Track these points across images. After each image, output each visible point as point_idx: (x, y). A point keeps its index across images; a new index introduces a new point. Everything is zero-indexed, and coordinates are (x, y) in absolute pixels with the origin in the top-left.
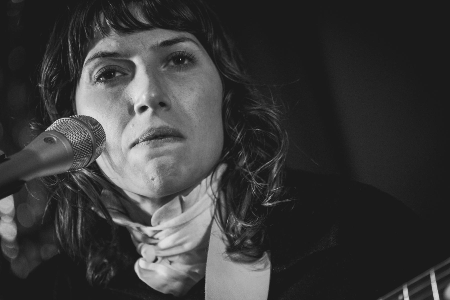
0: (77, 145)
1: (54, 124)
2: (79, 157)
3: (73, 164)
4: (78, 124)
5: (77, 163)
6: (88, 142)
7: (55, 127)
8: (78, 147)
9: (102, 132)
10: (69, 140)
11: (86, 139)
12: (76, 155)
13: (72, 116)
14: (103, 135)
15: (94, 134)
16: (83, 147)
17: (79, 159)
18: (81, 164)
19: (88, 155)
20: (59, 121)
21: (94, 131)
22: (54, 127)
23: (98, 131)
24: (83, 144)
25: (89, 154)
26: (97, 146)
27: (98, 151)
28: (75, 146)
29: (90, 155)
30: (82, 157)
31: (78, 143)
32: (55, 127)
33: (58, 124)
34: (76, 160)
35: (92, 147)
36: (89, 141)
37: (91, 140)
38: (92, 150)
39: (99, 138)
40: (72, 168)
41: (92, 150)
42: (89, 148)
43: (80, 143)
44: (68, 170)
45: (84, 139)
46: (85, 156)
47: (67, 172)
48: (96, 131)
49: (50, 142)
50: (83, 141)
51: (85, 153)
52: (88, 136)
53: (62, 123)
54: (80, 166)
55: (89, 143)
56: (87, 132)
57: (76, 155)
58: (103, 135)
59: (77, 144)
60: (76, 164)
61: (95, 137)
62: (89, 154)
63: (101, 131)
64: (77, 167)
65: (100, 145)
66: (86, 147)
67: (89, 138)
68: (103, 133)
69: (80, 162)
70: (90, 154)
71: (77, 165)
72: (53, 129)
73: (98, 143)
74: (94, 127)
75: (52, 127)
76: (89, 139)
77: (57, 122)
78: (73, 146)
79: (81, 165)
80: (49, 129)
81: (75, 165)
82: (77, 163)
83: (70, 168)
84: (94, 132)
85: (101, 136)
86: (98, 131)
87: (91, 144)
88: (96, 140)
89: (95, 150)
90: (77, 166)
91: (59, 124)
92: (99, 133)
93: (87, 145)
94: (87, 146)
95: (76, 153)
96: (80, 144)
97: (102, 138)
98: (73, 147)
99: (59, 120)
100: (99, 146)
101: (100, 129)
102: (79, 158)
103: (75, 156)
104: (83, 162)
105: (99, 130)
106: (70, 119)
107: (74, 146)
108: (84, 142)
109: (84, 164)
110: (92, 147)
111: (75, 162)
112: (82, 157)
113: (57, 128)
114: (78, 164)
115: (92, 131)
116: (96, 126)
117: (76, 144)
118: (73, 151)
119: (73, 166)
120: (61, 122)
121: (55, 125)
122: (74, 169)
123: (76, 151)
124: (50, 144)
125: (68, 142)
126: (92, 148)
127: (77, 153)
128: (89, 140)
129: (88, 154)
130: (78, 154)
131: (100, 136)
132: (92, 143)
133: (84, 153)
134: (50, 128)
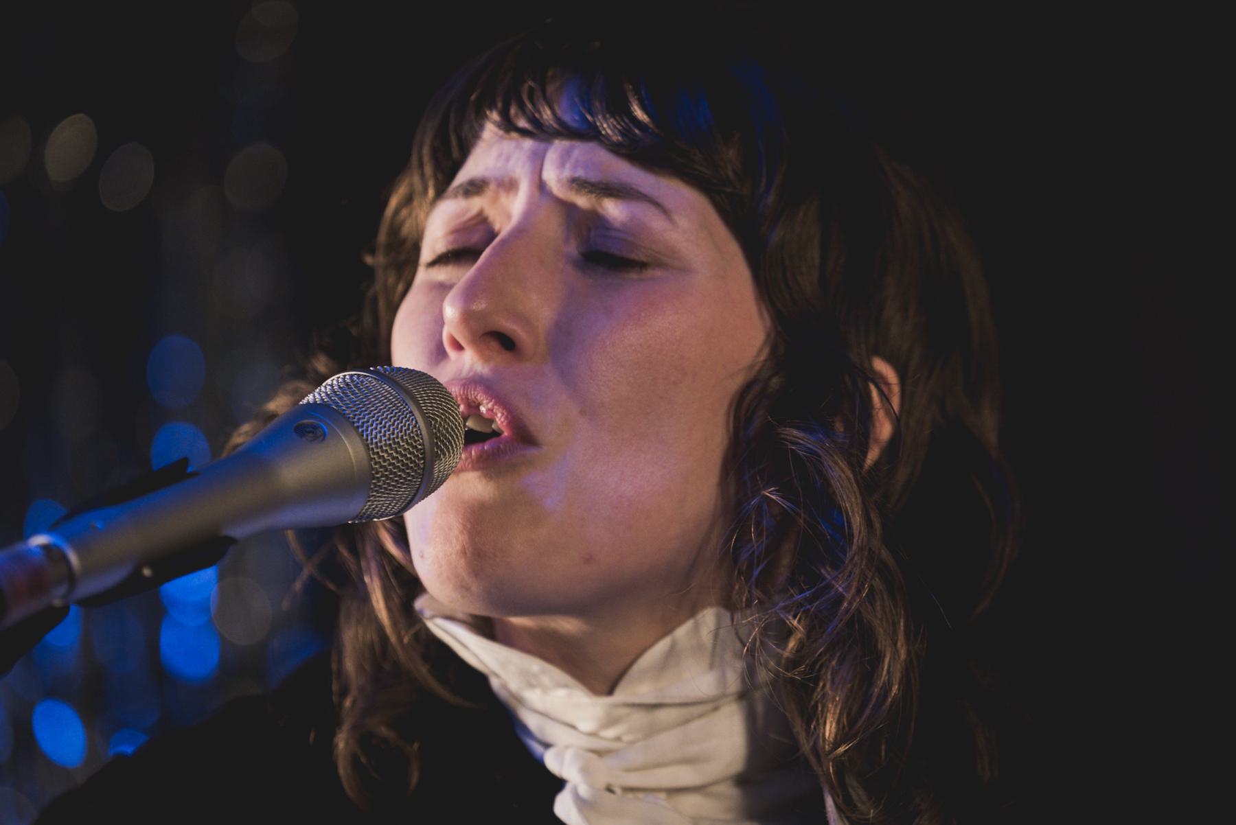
0: (382, 451)
1: (326, 388)
2: (384, 484)
3: (369, 501)
5: (379, 501)
6: (414, 444)
7: (327, 395)
9: (454, 418)
10: (363, 435)
11: (409, 434)
12: (378, 478)
13: (375, 367)
14: (456, 428)
15: (433, 422)
16: (400, 458)
18: (390, 504)
20: (340, 380)
21: (432, 414)
23: (442, 414)
24: (399, 450)
26: (438, 456)
28: (378, 453)
29: (415, 482)
31: (386, 445)
32: (327, 395)
34: (378, 492)
36: (415, 441)
37: (422, 439)
38: (422, 466)
39: (443, 435)
40: (364, 514)
41: (423, 469)
42: (415, 461)
43: (390, 444)
44: (354, 519)
45: (402, 436)
47: (350, 522)
48: (438, 416)
49: (311, 435)
50: (399, 440)
52: (415, 426)
53: (347, 385)
54: (386, 509)
55: (416, 447)
56: (413, 415)
58: (456, 428)
59: (384, 448)
60: (375, 503)
61: (434, 431)
63: (451, 415)
64: (384, 512)
65: (445, 455)
66: (407, 459)
67: (419, 432)
68: (457, 421)
69: (387, 497)
70: (417, 478)
71: (377, 507)
72: (322, 399)
73: (442, 450)
74: (434, 403)
75: (320, 394)
76: (417, 435)
77: (335, 382)
78: (371, 452)
79: (388, 507)
81: (373, 506)
82: (379, 501)
83: (360, 513)
84: (433, 419)
85: (450, 430)
86: (442, 414)
87: (421, 449)
88: (435, 441)
89: (432, 468)
90: (377, 509)
91: (340, 388)
92: (447, 420)
93: (410, 453)
94: (409, 456)
95: (377, 473)
96: (392, 449)
97: (452, 437)
98: (372, 456)
99: (341, 375)
101: (450, 409)
103: (374, 481)
105: (446, 412)
106: (372, 377)
107: (374, 454)
108: (401, 444)
109: (396, 503)
110: (423, 459)
111: (373, 496)
113: (333, 398)
114: (381, 503)
115: (427, 413)
116: (439, 401)
117: (381, 447)
119: (367, 507)
120: (344, 381)
122: (369, 516)
124: (311, 441)
125: (358, 439)
126: (422, 462)
127: (381, 471)
128: (416, 438)
130: (381, 477)
131: (448, 429)
132: (424, 449)
133: (399, 473)
134: (314, 396)
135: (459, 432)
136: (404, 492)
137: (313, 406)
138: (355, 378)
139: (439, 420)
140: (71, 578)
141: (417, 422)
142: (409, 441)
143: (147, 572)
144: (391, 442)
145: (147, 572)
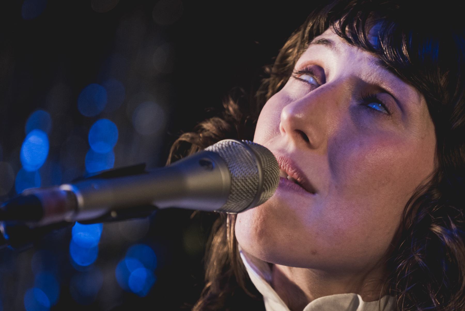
1: (219, 145)
4: (249, 155)
8: (239, 184)
14: (276, 179)
15: (266, 174)
17: (235, 200)
19: (248, 199)
20: (227, 143)
22: (217, 148)
23: (271, 170)
25: (250, 197)
27: (263, 197)
30: (240, 200)
33: (224, 146)
34: (231, 200)
35: (257, 190)
38: (255, 193)
41: (256, 195)
43: (242, 180)
44: (217, 210)
46: (244, 199)
51: (245, 195)
52: (257, 174)
53: (229, 146)
57: (233, 195)
62: (250, 197)
63: (275, 171)
65: (267, 190)
72: (216, 150)
75: (215, 148)
76: (257, 178)
80: (210, 148)
81: (228, 207)
86: (271, 170)
89: (260, 195)
91: (225, 146)
100: (266, 191)
102: (236, 199)
103: (231, 195)
104: (238, 205)
105: (273, 169)
112: (240, 200)
118: (231, 187)
121: (220, 145)
123: (234, 189)
127: (235, 192)
129: (248, 198)
135: (277, 180)
136: (244, 203)
137: (211, 153)
138: (234, 144)
139: (269, 173)
140: (76, 208)
141: (258, 172)
142: (252, 180)
143: (113, 214)
144: (243, 178)
145: (113, 214)
